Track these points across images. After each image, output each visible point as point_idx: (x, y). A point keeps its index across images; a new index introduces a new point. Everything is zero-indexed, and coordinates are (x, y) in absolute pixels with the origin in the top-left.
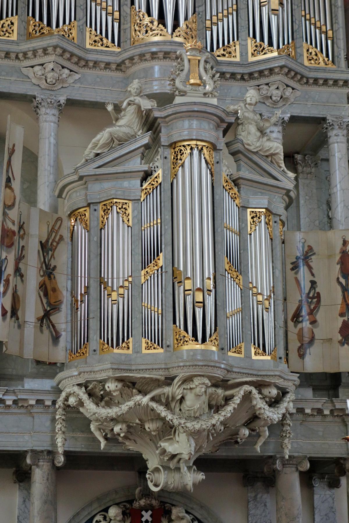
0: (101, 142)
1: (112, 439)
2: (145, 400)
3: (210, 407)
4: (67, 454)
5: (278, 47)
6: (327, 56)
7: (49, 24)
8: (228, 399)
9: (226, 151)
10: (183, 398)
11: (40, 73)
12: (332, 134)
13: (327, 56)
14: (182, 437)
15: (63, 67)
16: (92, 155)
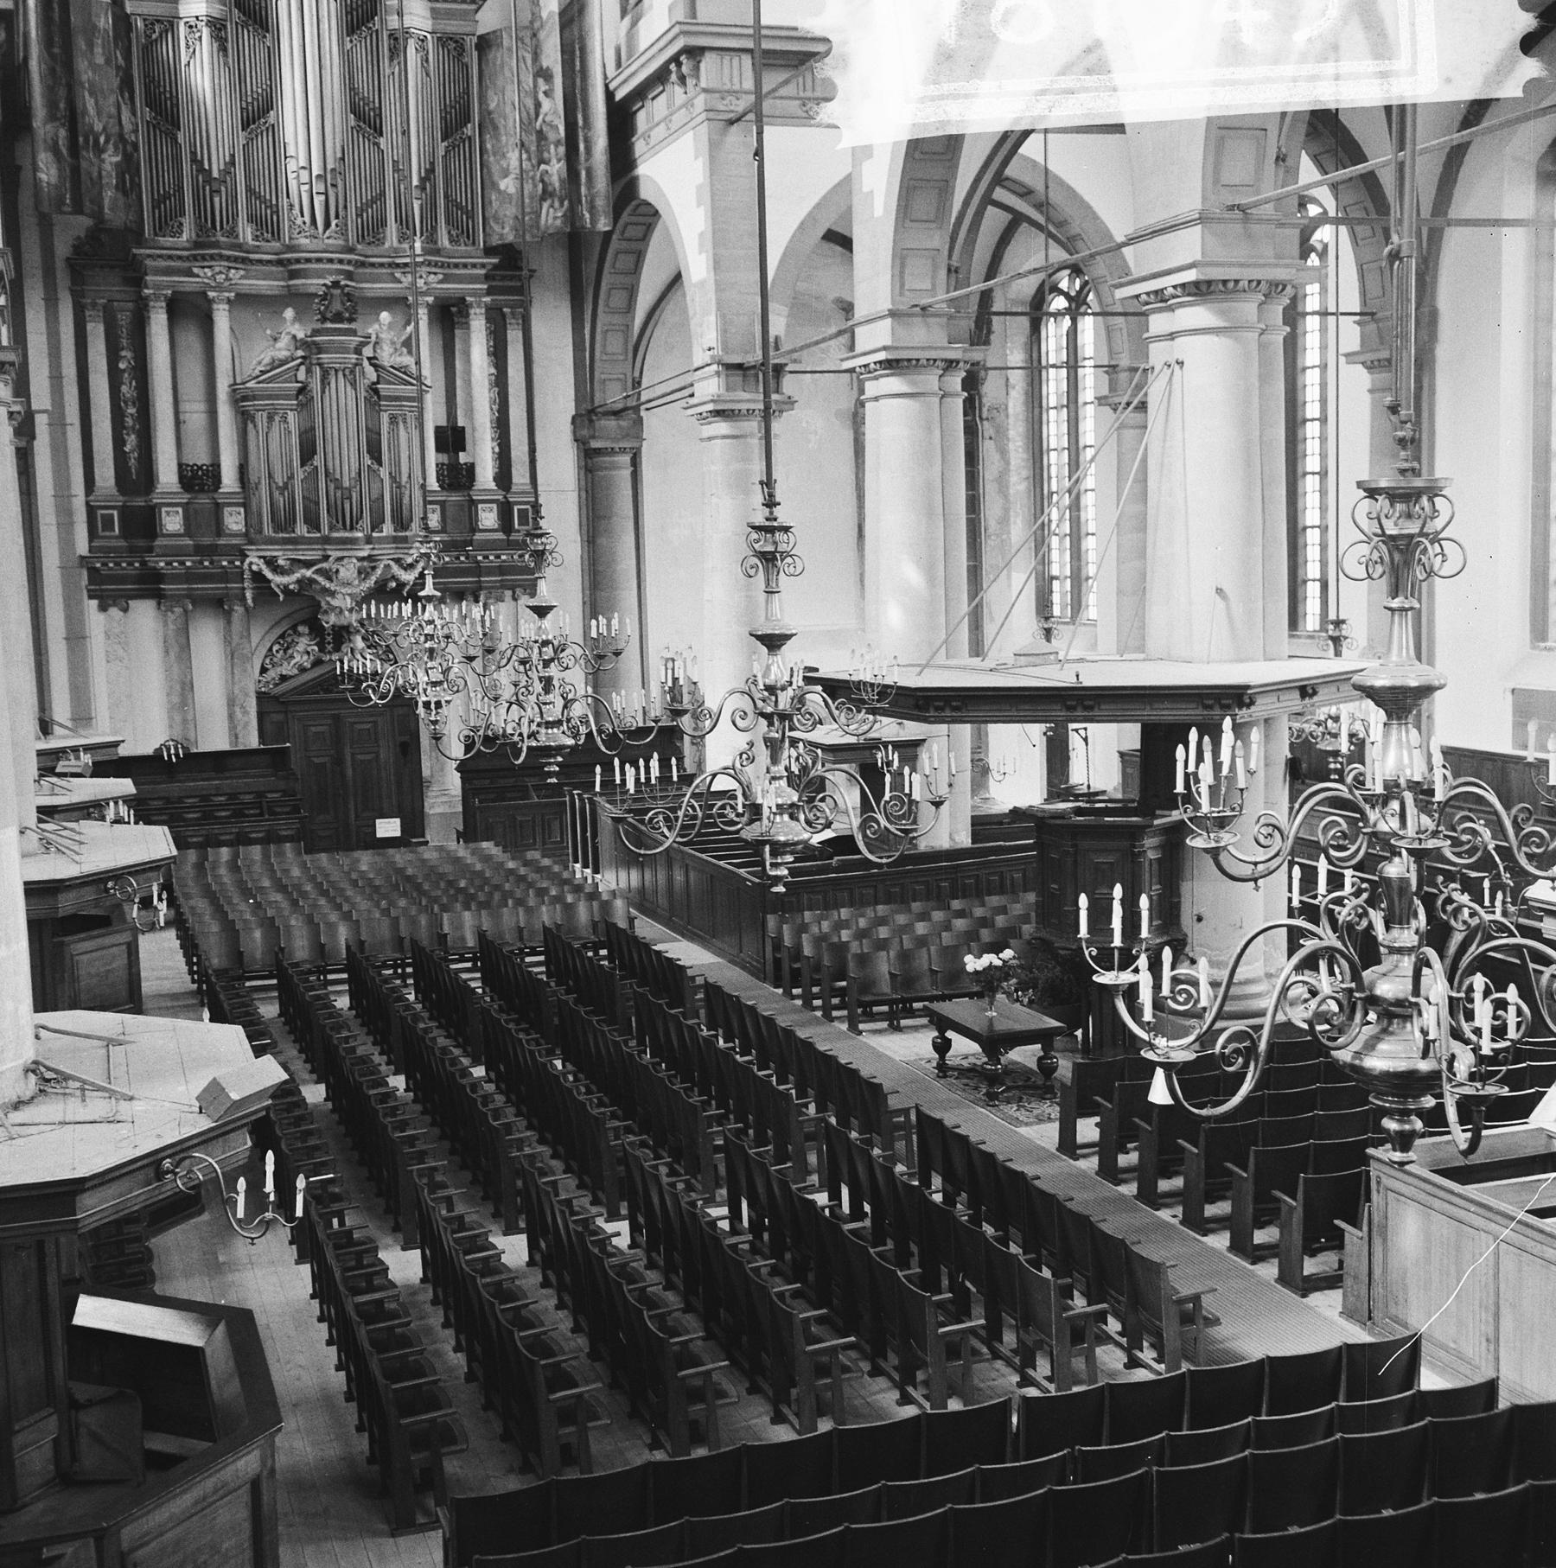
0: (265, 362)
1: (286, 590)
2: (309, 573)
3: (360, 573)
4: (254, 599)
5: (422, 235)
6: (468, 238)
7: (214, 226)
8: (374, 568)
9: (366, 363)
10: (337, 571)
11: (209, 274)
12: (472, 311)
13: (468, 238)
14: (339, 596)
15: (230, 268)
16: (257, 372)
